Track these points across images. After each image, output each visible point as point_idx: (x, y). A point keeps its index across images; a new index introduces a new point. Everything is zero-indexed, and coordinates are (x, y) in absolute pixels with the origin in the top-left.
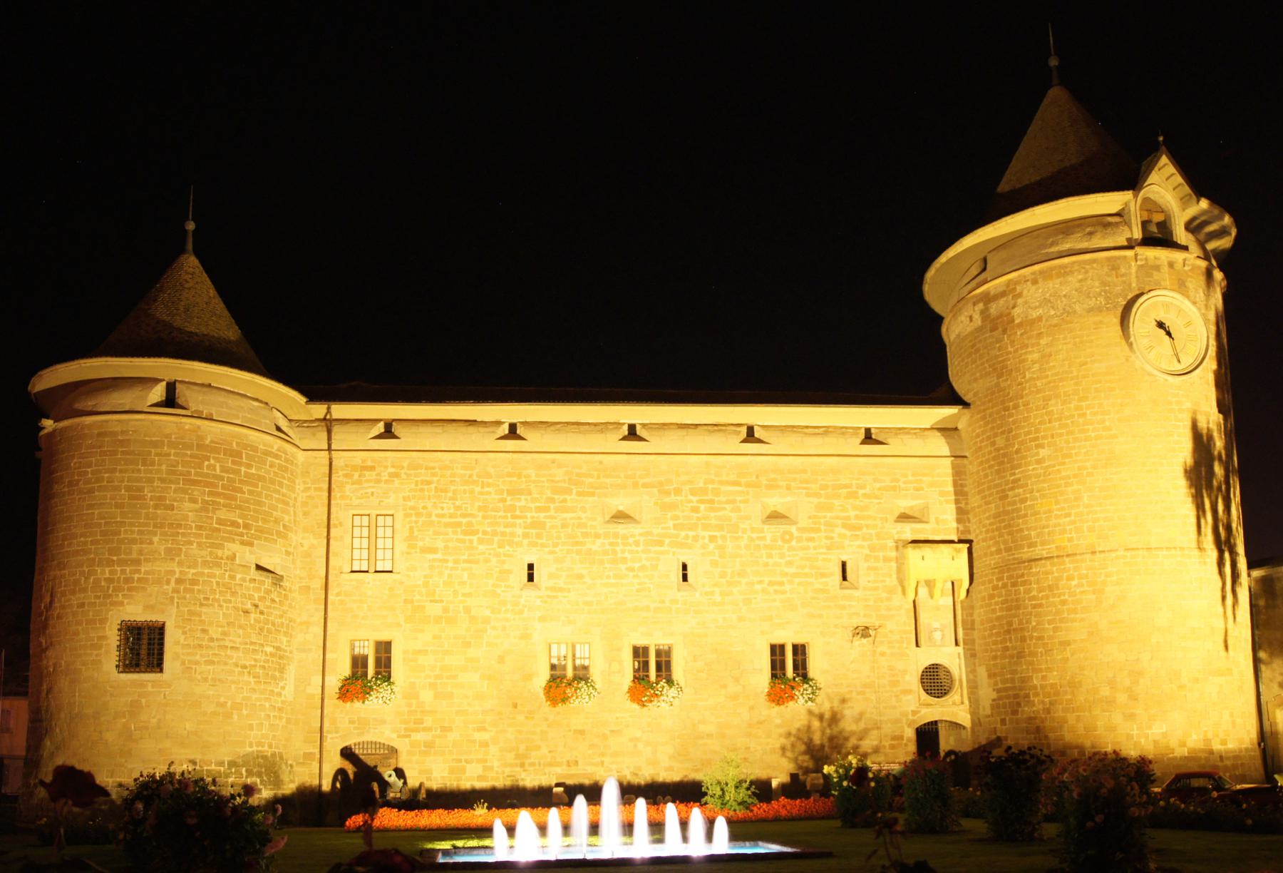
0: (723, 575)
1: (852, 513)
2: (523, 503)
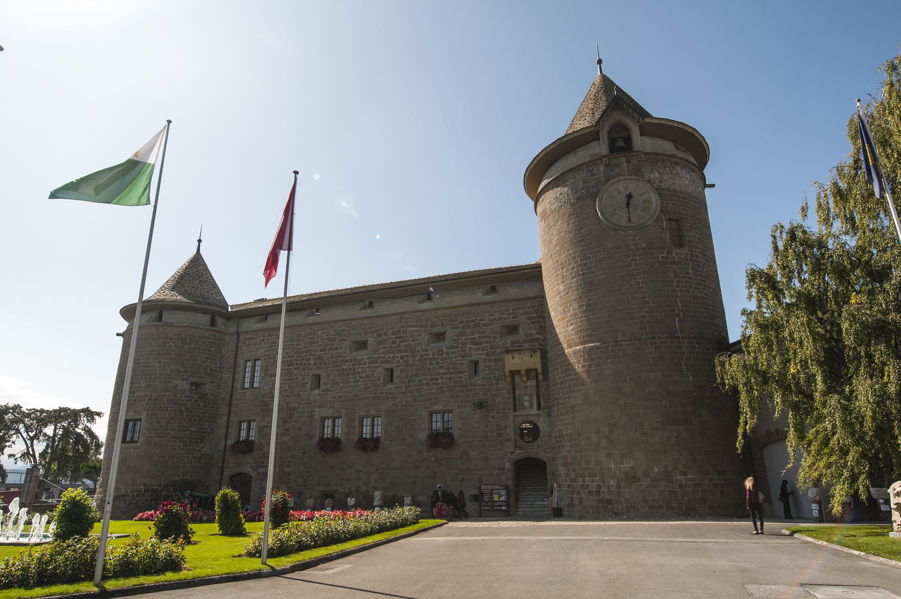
0: (407, 376)
1: (477, 336)
2: (314, 348)
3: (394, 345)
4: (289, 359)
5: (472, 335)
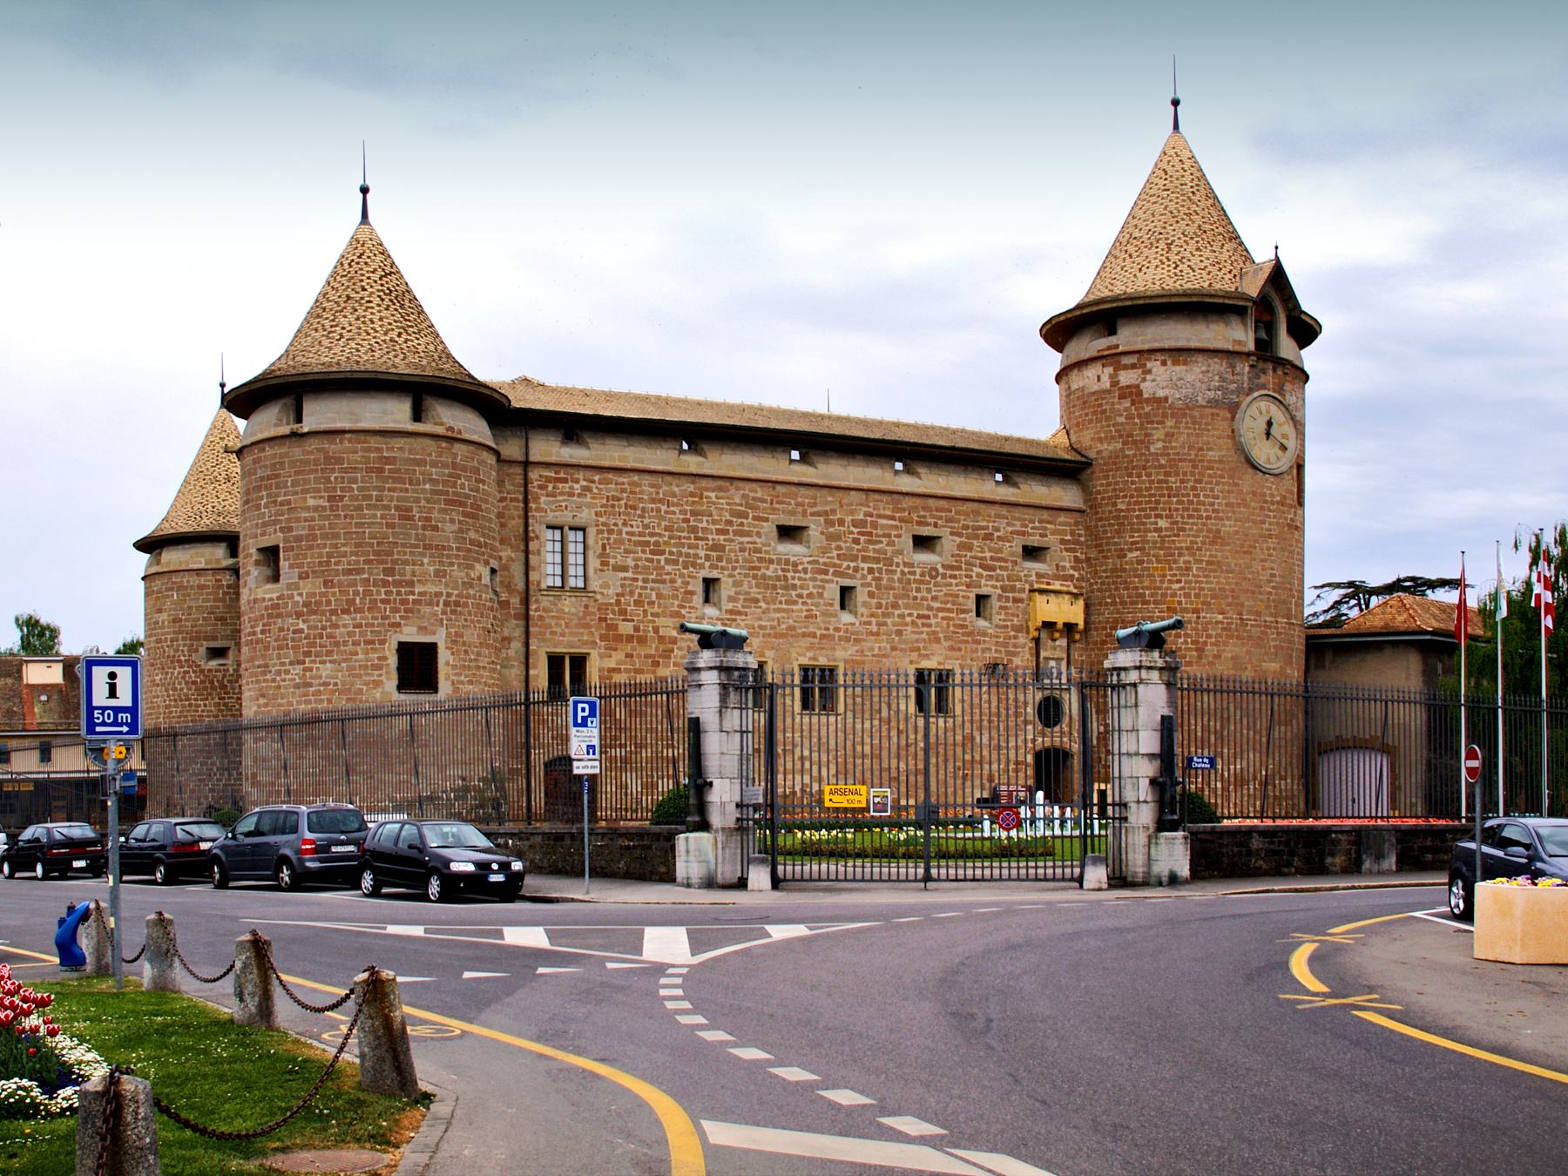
0: (879, 606)
1: (988, 555)
2: (704, 525)
3: (857, 547)
4: (652, 540)
5: (981, 552)
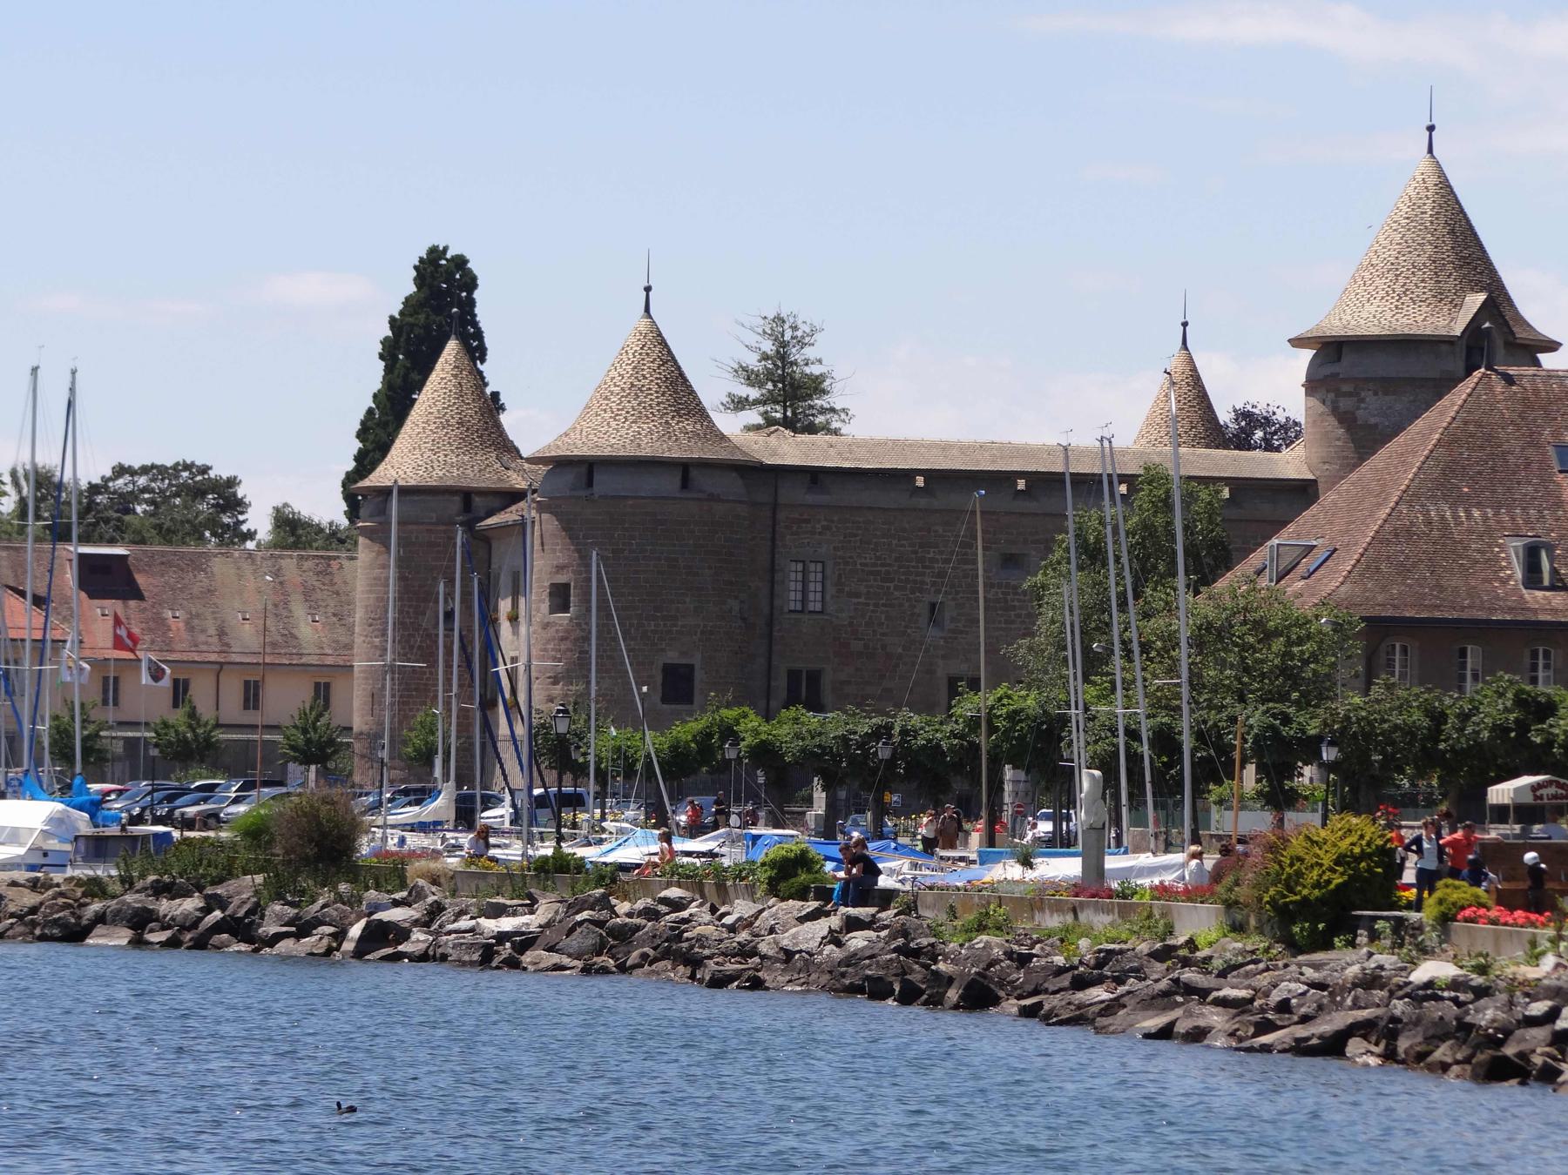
2: (931, 555)
